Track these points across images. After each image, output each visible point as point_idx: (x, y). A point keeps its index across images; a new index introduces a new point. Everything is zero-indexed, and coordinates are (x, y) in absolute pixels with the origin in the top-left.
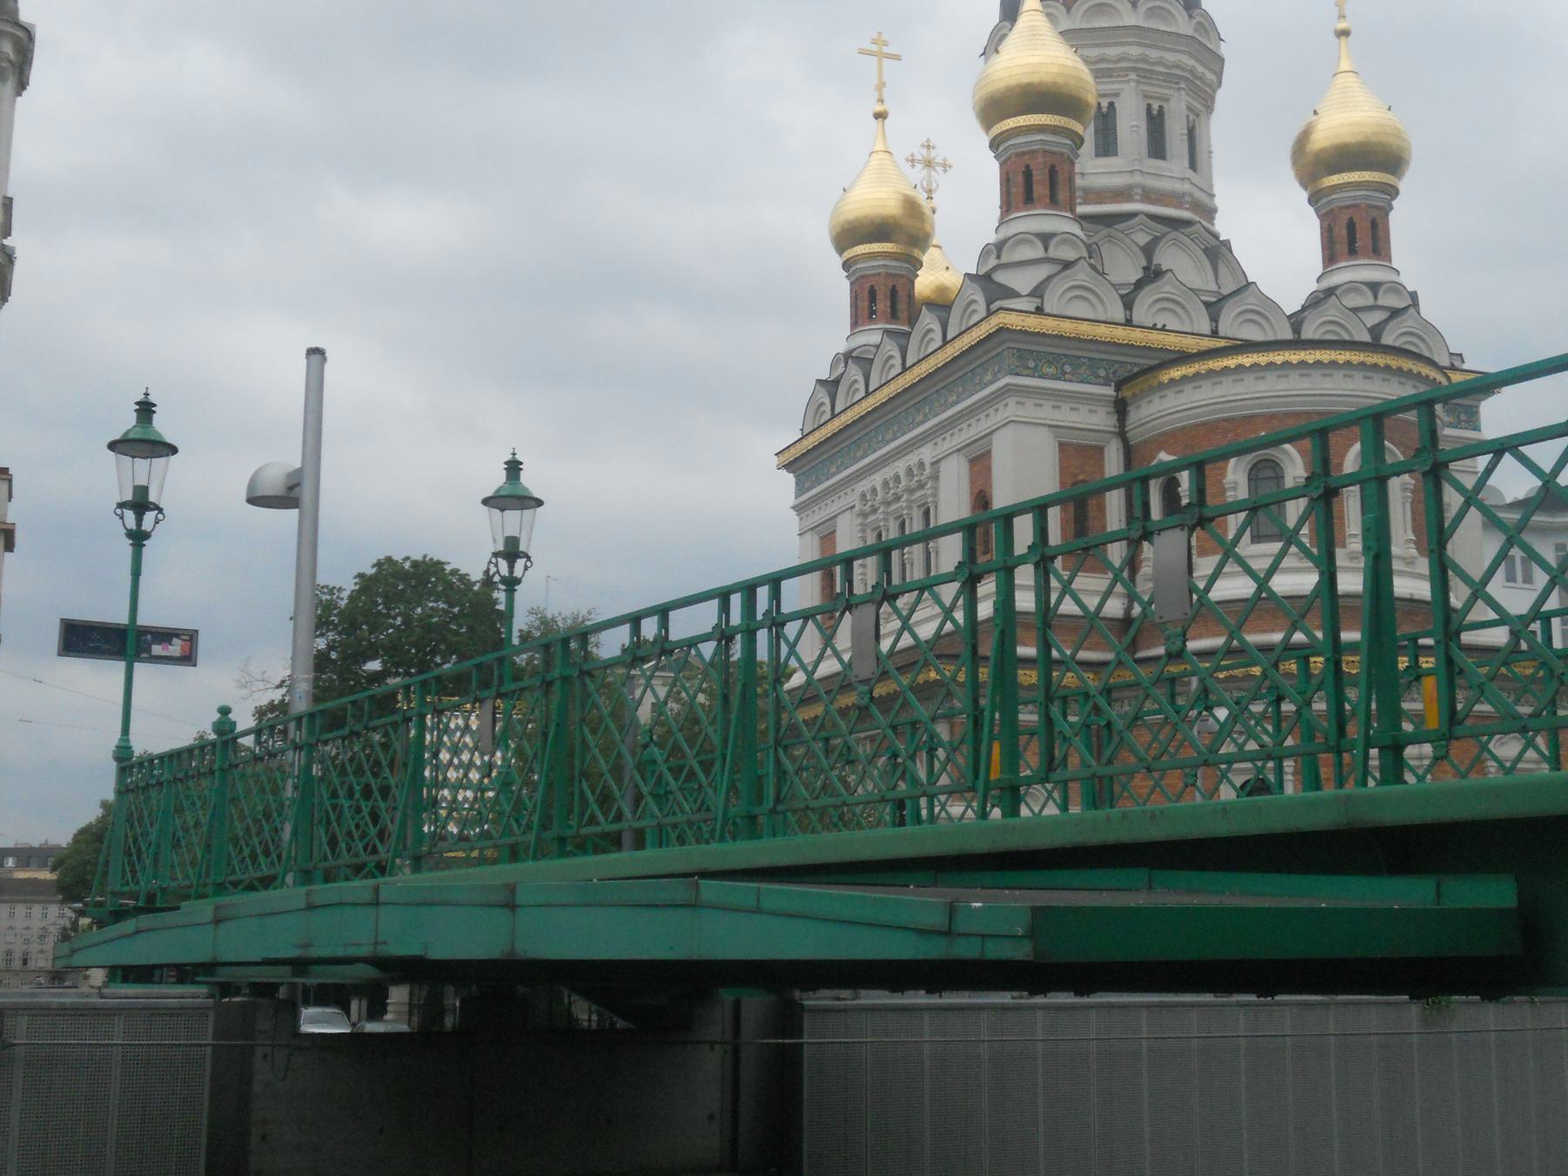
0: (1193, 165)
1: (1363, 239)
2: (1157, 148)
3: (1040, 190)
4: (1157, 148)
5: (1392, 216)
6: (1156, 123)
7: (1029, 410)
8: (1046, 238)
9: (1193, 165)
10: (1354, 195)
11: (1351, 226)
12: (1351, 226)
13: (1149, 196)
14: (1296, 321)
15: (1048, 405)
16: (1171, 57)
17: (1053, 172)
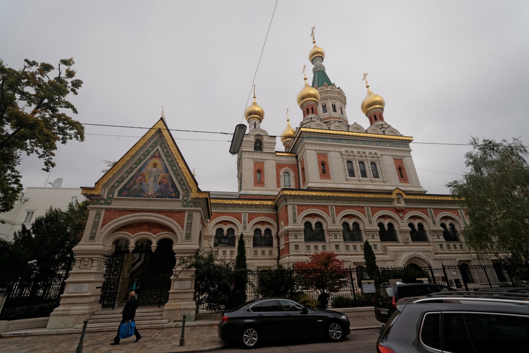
0: (342, 114)
1: (378, 117)
2: (335, 110)
3: (310, 111)
4: (335, 110)
5: (383, 115)
6: (334, 107)
7: (310, 147)
8: (311, 118)
9: (342, 114)
10: (374, 111)
11: (375, 116)
12: (375, 116)
13: (334, 118)
14: (366, 131)
15: (314, 146)
16: (336, 95)
17: (312, 108)
